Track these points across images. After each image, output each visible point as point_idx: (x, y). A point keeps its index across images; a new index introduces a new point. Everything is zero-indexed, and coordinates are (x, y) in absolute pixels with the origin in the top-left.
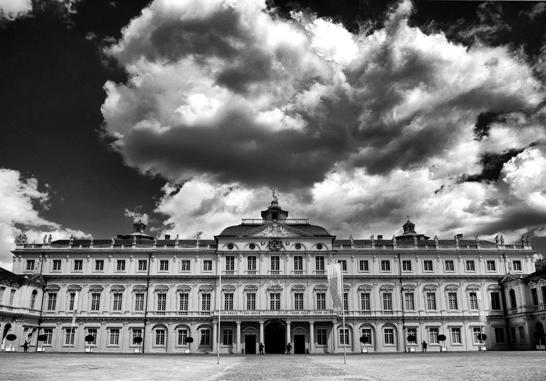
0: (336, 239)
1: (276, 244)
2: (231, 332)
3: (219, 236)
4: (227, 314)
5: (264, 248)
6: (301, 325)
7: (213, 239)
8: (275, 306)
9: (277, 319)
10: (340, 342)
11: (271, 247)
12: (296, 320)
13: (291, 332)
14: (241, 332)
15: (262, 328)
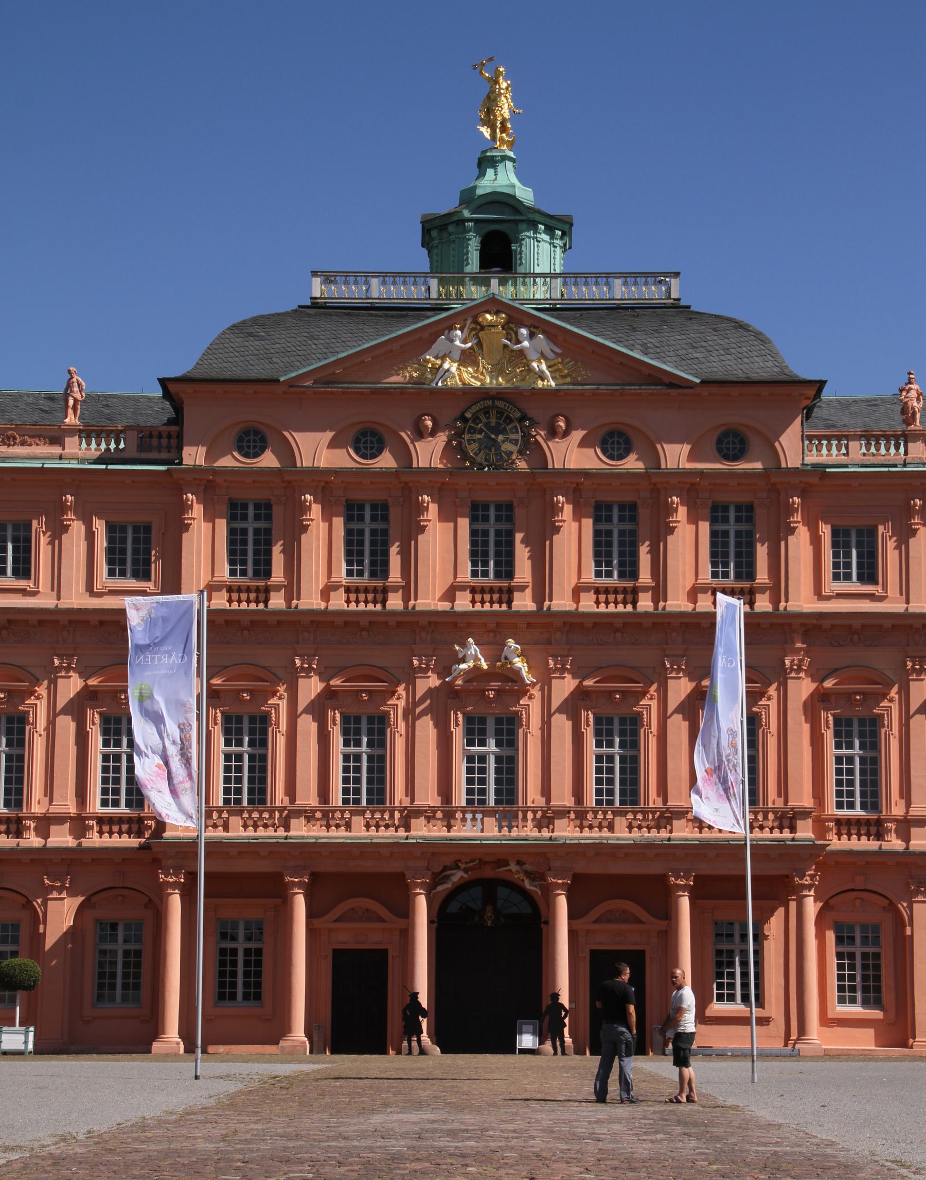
0: (826, 395)
1: (498, 430)
2: (255, 931)
3: (184, 380)
4: (238, 831)
5: (429, 453)
6: (626, 889)
7: (158, 392)
8: (491, 786)
9: (502, 862)
10: (833, 993)
11: (472, 449)
12: (596, 868)
13: (571, 932)
14: (311, 931)
15: (422, 904)
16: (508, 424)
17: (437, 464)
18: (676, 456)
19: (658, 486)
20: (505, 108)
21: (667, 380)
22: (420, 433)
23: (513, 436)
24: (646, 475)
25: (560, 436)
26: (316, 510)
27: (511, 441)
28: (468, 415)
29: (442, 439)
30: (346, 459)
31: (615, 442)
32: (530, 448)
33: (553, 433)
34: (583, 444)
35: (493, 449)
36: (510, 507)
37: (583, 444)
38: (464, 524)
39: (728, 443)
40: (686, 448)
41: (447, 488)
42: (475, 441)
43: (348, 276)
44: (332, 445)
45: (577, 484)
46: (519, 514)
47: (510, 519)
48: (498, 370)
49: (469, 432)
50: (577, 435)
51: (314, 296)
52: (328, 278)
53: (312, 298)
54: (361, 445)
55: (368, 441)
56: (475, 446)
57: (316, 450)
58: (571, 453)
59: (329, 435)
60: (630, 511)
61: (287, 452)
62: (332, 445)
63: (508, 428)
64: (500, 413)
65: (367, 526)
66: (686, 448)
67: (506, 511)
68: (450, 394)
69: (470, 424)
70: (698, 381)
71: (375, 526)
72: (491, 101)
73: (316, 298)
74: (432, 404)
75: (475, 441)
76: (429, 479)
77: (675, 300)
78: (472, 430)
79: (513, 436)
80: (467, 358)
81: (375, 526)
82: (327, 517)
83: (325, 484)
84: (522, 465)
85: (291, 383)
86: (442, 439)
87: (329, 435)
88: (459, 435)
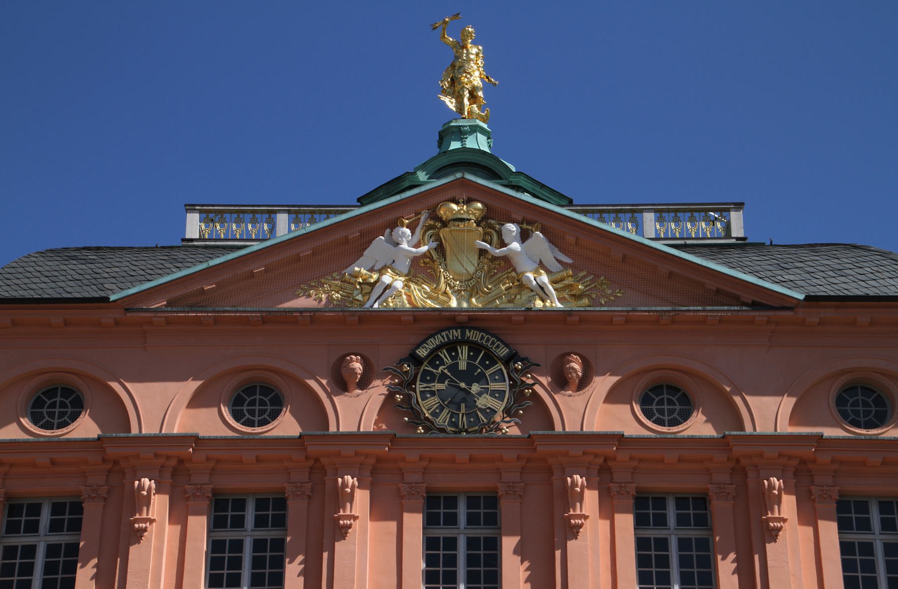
1: (470, 376)
11: (427, 406)
16: (487, 367)
17: (369, 425)
18: (770, 414)
19: (744, 463)
20: (475, 77)
21: (747, 297)
22: (341, 383)
23: (494, 386)
24: (722, 443)
25: (574, 387)
26: (159, 505)
27: (493, 394)
28: (422, 352)
29: (378, 390)
30: (214, 423)
31: (664, 397)
32: (524, 403)
33: (561, 382)
34: (612, 397)
35: (463, 406)
36: (492, 501)
37: (612, 397)
38: (414, 522)
39: (856, 403)
40: (788, 403)
41: (382, 465)
42: (433, 393)
43: (240, 213)
44: (197, 401)
45: (604, 458)
46: (507, 508)
47: (492, 520)
48: (471, 287)
49: (423, 380)
50: (603, 384)
51: (188, 236)
52: (209, 215)
53: (184, 240)
54: (245, 408)
55: (255, 398)
56: (433, 401)
57: (165, 407)
58: (593, 410)
59: (192, 386)
60: (696, 508)
61: (116, 413)
62: (197, 401)
63: (488, 373)
64: (475, 348)
65: (249, 535)
66: (788, 403)
67: (486, 509)
68: (395, 320)
69: (425, 367)
70: (801, 297)
71: (261, 534)
72: (456, 68)
73: (192, 240)
74: (362, 336)
75: (433, 393)
76: (357, 451)
77: (738, 239)
78: (429, 377)
79: (494, 386)
80: (421, 270)
81: (261, 534)
82: (178, 515)
83: (179, 464)
84: (512, 430)
85: (128, 305)
86: (378, 390)
87: (192, 386)
88: (408, 384)
